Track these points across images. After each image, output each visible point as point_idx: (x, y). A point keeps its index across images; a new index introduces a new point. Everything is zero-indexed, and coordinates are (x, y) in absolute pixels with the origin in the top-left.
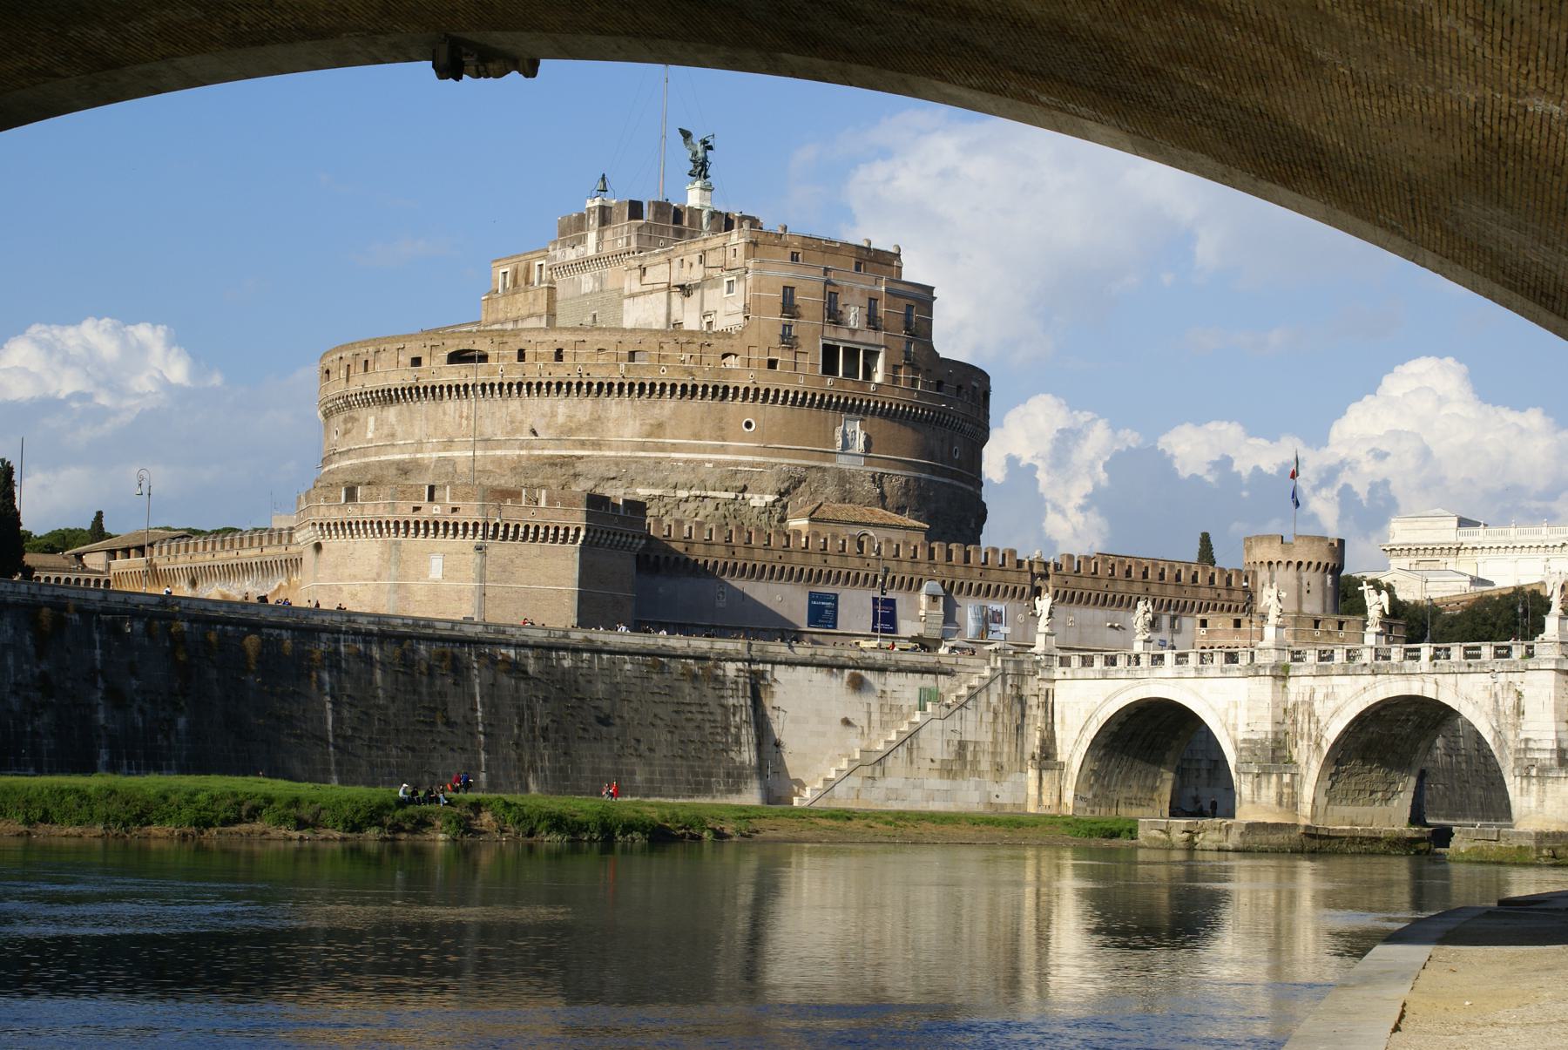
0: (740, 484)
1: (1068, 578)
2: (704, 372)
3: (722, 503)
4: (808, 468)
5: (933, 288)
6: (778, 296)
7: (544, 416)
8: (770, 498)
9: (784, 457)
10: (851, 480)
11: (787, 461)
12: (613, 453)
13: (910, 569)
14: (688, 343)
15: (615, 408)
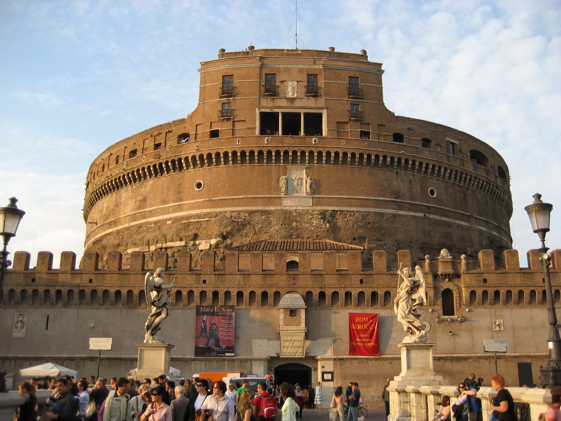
0: (191, 233)
1: (486, 276)
3: (177, 250)
4: (251, 213)
6: (218, 84)
7: (100, 211)
8: (213, 242)
9: (229, 206)
12: (120, 227)
15: (126, 193)
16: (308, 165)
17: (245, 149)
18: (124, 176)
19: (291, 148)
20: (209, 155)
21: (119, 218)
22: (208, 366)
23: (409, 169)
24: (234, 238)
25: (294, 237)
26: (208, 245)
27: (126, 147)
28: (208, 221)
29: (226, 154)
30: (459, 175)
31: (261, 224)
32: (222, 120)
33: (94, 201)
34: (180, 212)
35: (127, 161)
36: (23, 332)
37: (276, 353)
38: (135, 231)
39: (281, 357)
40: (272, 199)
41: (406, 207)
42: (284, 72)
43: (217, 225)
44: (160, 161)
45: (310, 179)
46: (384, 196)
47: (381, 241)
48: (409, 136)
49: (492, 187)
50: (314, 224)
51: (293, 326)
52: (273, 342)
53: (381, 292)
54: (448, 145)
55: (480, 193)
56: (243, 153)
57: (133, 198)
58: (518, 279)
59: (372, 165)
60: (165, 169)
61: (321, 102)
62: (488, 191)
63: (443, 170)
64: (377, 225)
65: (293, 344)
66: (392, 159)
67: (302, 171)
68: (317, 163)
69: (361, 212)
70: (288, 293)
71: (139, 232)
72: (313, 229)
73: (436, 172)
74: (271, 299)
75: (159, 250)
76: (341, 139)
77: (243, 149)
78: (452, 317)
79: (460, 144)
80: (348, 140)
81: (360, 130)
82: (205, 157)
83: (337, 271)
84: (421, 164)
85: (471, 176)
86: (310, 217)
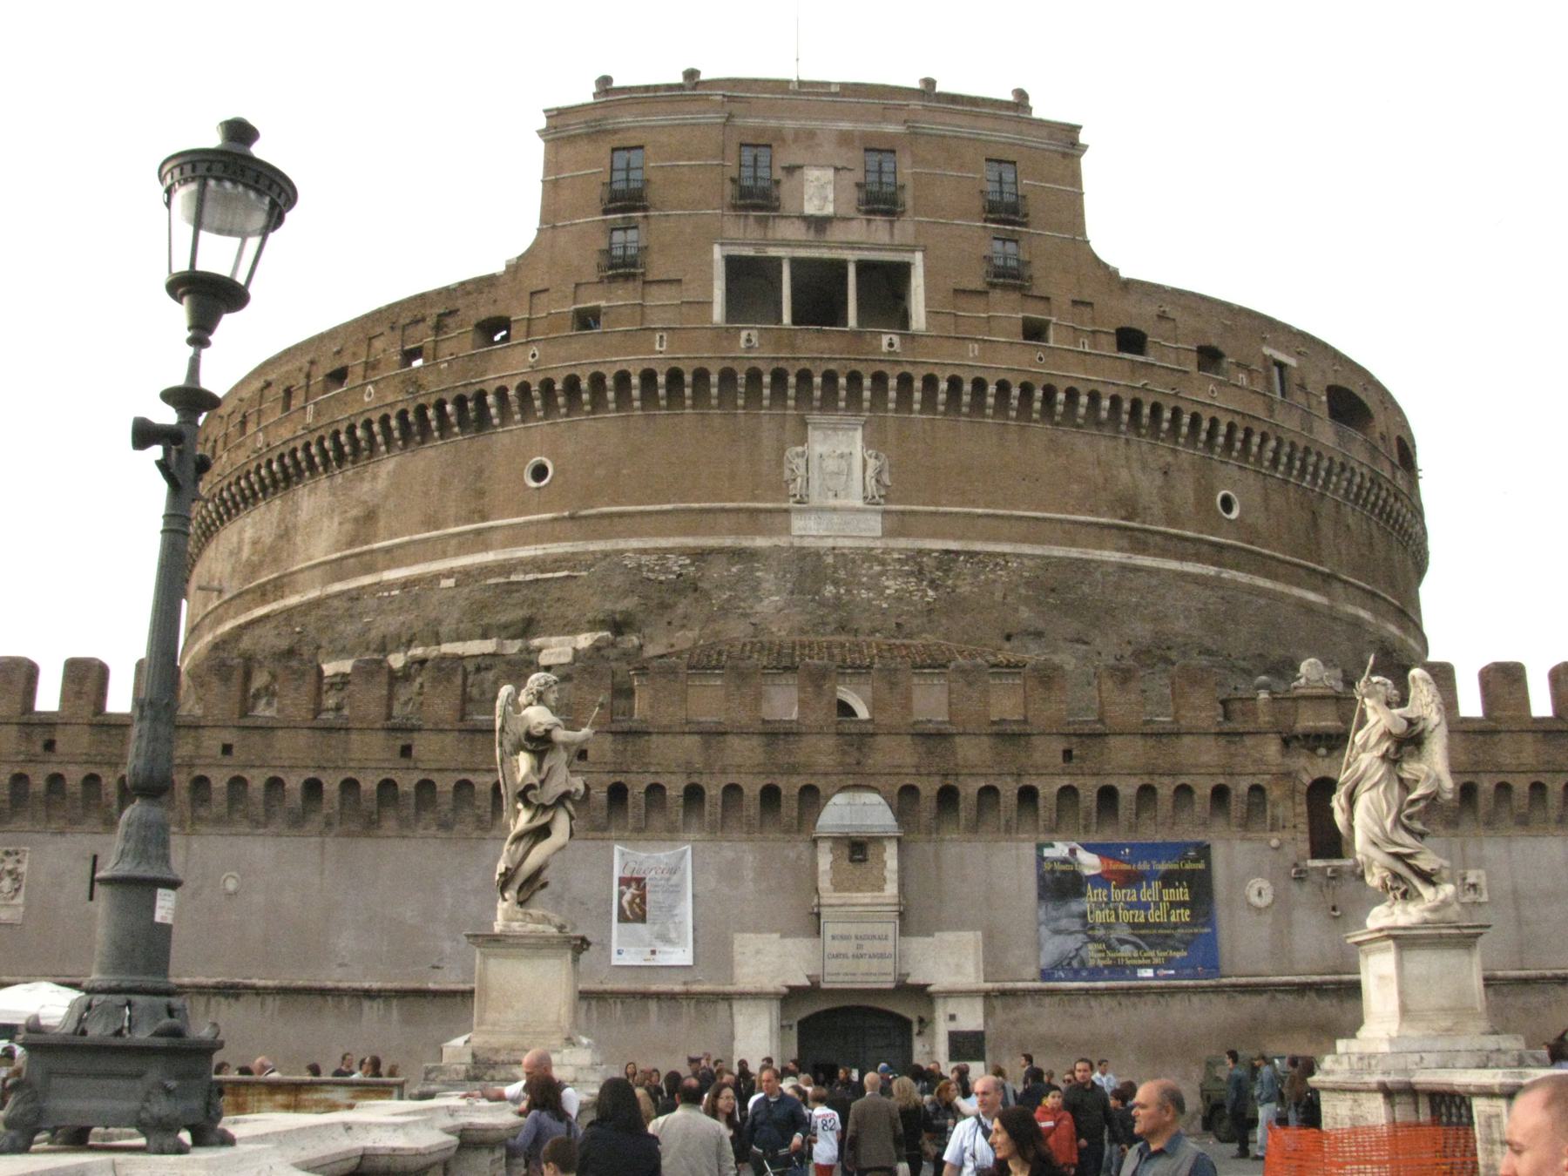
2: (440, 372)
3: (470, 667)
4: (699, 555)
5: (1074, 129)
7: (231, 553)
8: (584, 641)
10: (842, 574)
11: (635, 543)
12: (293, 600)
13: (759, 756)
14: (417, 321)
16: (867, 414)
17: (680, 365)
18: (307, 446)
19: (818, 362)
20: (572, 384)
21: (292, 573)
22: (595, 1015)
23: (1162, 435)
24: (647, 631)
25: (829, 629)
26: (570, 650)
27: (312, 363)
28: (568, 577)
29: (623, 378)
30: (1299, 455)
31: (730, 590)
32: (608, 277)
33: (214, 523)
34: (480, 551)
35: (315, 404)
36: (16, 906)
37: (808, 977)
38: (340, 612)
39: (824, 986)
40: (762, 517)
41: (1156, 546)
42: (796, 139)
43: (595, 593)
44: (421, 401)
45: (876, 458)
46: (1093, 511)
47: (1086, 643)
48: (1161, 337)
49: (1384, 494)
50: (888, 591)
51: (861, 891)
52: (797, 940)
53: (1127, 789)
54: (1268, 369)
55: (1354, 510)
56: (675, 377)
57: (333, 511)
58: (1528, 751)
59: (1057, 418)
60: (434, 424)
61: (905, 229)
62: (1374, 505)
63: (1256, 440)
64: (1073, 596)
65: (859, 947)
66: (1116, 401)
67: (851, 433)
68: (896, 411)
69: (1026, 556)
70: (843, 789)
71: (353, 612)
72: (885, 606)
73: (1238, 445)
74: (789, 808)
75: (416, 666)
76: (967, 342)
77: (674, 364)
78: (1336, 862)
79: (1299, 368)
80: (987, 344)
81: (1020, 315)
82: (558, 386)
83: (994, 723)
84: (1196, 419)
85: (1331, 459)
86: (877, 568)
